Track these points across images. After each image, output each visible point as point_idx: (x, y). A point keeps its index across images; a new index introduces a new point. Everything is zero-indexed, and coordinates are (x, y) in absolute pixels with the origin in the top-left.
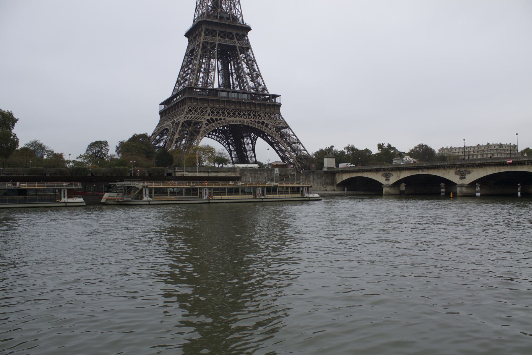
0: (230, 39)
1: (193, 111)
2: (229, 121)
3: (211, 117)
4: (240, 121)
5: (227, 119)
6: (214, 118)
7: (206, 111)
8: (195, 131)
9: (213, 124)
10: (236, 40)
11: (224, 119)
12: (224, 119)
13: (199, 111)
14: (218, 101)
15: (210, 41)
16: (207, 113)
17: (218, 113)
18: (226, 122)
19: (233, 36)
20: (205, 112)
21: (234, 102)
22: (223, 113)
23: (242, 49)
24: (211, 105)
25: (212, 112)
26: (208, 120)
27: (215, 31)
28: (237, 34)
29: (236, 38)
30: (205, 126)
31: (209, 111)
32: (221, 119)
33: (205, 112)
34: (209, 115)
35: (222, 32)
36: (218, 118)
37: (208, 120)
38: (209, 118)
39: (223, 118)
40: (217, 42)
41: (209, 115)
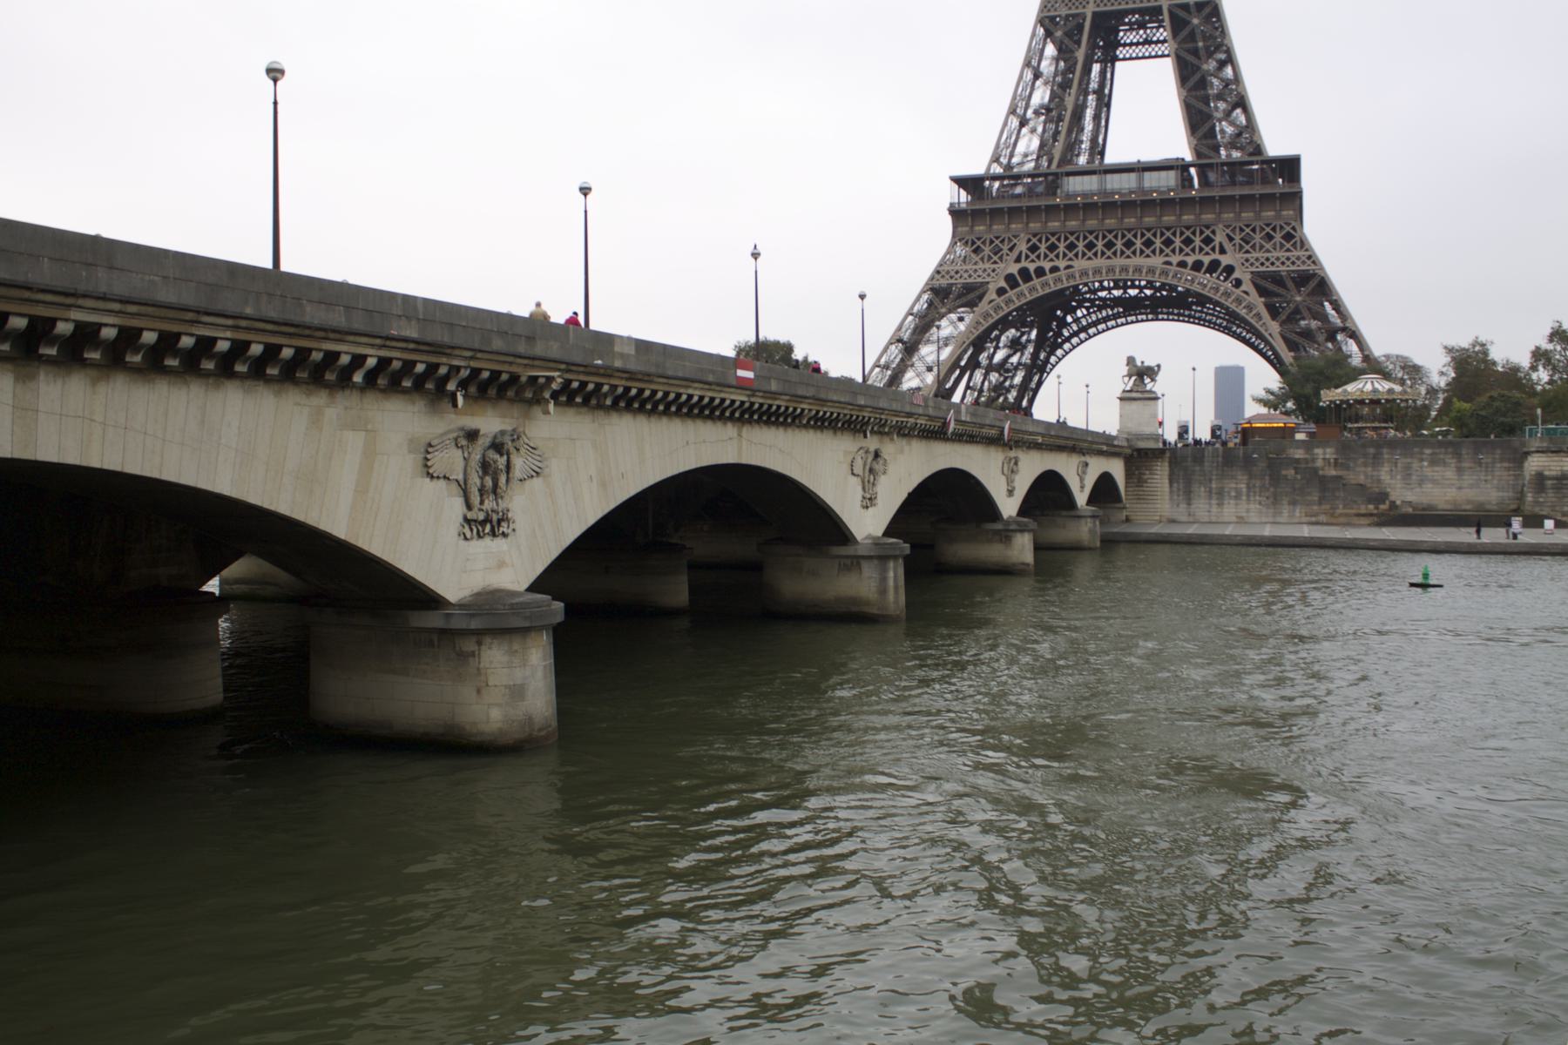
2: (1084, 273)
3: (1024, 264)
4: (1124, 269)
5: (1080, 264)
6: (1032, 267)
7: (1011, 249)
9: (1024, 287)
12: (1068, 267)
13: (987, 250)
14: (1051, 210)
17: (1052, 248)
18: (1072, 276)
20: (1006, 250)
21: (1127, 205)
22: (1071, 247)
23: (1182, 14)
25: (1034, 249)
26: (1010, 279)
30: (994, 296)
31: (1023, 247)
32: (1054, 269)
33: (1006, 250)
34: (1018, 260)
36: (1047, 266)
37: (1010, 279)
38: (1014, 269)
39: (1062, 264)
40: (1089, 11)
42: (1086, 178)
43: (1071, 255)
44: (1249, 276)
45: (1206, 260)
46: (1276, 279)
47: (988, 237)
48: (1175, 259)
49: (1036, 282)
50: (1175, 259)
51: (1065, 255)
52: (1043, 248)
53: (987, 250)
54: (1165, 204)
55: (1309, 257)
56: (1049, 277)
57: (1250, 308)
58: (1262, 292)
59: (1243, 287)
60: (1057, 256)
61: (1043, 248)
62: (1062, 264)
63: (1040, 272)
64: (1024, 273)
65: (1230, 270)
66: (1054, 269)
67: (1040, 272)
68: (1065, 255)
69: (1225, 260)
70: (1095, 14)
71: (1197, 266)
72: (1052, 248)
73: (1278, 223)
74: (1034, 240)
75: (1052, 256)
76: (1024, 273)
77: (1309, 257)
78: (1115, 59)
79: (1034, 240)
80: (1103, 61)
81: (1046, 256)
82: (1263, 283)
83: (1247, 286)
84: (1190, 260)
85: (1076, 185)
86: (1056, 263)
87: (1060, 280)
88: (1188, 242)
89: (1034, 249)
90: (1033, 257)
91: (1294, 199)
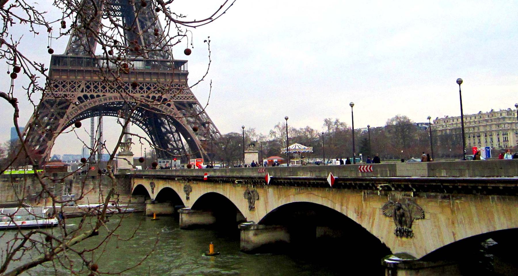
1: (60, 86)
2: (110, 98)
3: (85, 93)
5: (108, 95)
7: (79, 87)
8: (59, 114)
11: (104, 95)
12: (104, 95)
13: (69, 86)
16: (80, 89)
17: (96, 87)
20: (76, 87)
24: (88, 78)
25: (88, 87)
26: (79, 98)
31: (83, 86)
32: (98, 96)
33: (76, 87)
34: (82, 91)
36: (95, 95)
37: (79, 98)
38: (81, 95)
39: (101, 94)
41: (82, 91)
43: (104, 91)
44: (172, 103)
45: (157, 96)
46: (182, 104)
47: (68, 81)
48: (145, 95)
50: (145, 95)
53: (69, 86)
54: (141, 73)
55: (193, 97)
57: (175, 114)
58: (179, 109)
59: (171, 107)
60: (99, 90)
62: (101, 94)
64: (86, 97)
65: (165, 100)
66: (98, 96)
67: (92, 97)
68: (102, 91)
69: (164, 97)
71: (154, 98)
72: (96, 87)
73: (180, 84)
74: (88, 84)
75: (96, 90)
76: (86, 97)
77: (193, 97)
79: (88, 84)
82: (178, 105)
83: (173, 106)
84: (151, 96)
86: (98, 94)
87: (101, 100)
88: (149, 89)
89: (88, 87)
91: (186, 74)
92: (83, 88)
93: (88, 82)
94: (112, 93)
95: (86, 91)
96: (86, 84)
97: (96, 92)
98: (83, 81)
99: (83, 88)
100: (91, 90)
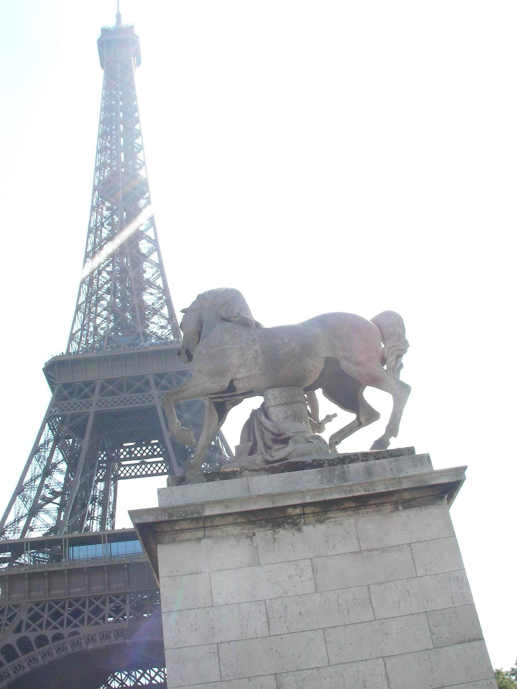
0: (139, 390)
6: (32, 636)
7: (10, 619)
9: (22, 658)
10: (155, 391)
15: (69, 413)
19: (147, 384)
25: (36, 617)
27: (87, 384)
28: (161, 376)
29: (157, 384)
31: (24, 616)
32: (58, 637)
34: (18, 630)
35: (110, 381)
36: (49, 634)
38: (12, 639)
39: (65, 631)
40: (92, 411)
42: (91, 547)
43: (76, 621)
49: (37, 651)
51: (69, 622)
52: (46, 616)
56: (52, 646)
61: (46, 616)
62: (65, 631)
63: (42, 641)
66: (58, 637)
67: (42, 641)
68: (69, 622)
70: (96, 412)
72: (56, 615)
74: (36, 609)
75: (55, 623)
78: (118, 478)
79: (36, 609)
80: (106, 480)
81: (48, 623)
85: (81, 553)
86: (60, 630)
87: (64, 648)
89: (36, 617)
90: (34, 625)
92: (21, 622)
93: (37, 605)
94: (97, 623)
95: (28, 626)
96: (31, 609)
97: (55, 628)
98: (24, 605)
99: (21, 622)
100: (41, 626)
